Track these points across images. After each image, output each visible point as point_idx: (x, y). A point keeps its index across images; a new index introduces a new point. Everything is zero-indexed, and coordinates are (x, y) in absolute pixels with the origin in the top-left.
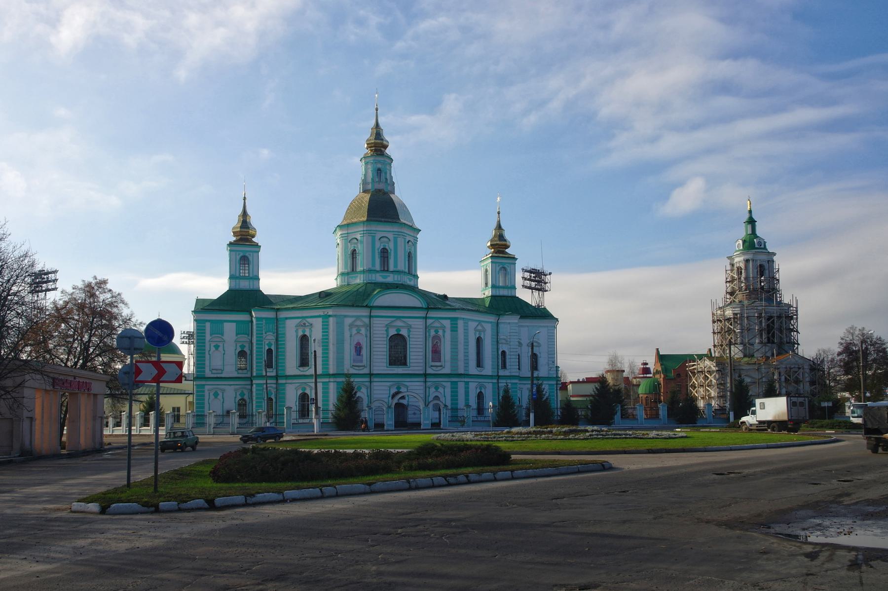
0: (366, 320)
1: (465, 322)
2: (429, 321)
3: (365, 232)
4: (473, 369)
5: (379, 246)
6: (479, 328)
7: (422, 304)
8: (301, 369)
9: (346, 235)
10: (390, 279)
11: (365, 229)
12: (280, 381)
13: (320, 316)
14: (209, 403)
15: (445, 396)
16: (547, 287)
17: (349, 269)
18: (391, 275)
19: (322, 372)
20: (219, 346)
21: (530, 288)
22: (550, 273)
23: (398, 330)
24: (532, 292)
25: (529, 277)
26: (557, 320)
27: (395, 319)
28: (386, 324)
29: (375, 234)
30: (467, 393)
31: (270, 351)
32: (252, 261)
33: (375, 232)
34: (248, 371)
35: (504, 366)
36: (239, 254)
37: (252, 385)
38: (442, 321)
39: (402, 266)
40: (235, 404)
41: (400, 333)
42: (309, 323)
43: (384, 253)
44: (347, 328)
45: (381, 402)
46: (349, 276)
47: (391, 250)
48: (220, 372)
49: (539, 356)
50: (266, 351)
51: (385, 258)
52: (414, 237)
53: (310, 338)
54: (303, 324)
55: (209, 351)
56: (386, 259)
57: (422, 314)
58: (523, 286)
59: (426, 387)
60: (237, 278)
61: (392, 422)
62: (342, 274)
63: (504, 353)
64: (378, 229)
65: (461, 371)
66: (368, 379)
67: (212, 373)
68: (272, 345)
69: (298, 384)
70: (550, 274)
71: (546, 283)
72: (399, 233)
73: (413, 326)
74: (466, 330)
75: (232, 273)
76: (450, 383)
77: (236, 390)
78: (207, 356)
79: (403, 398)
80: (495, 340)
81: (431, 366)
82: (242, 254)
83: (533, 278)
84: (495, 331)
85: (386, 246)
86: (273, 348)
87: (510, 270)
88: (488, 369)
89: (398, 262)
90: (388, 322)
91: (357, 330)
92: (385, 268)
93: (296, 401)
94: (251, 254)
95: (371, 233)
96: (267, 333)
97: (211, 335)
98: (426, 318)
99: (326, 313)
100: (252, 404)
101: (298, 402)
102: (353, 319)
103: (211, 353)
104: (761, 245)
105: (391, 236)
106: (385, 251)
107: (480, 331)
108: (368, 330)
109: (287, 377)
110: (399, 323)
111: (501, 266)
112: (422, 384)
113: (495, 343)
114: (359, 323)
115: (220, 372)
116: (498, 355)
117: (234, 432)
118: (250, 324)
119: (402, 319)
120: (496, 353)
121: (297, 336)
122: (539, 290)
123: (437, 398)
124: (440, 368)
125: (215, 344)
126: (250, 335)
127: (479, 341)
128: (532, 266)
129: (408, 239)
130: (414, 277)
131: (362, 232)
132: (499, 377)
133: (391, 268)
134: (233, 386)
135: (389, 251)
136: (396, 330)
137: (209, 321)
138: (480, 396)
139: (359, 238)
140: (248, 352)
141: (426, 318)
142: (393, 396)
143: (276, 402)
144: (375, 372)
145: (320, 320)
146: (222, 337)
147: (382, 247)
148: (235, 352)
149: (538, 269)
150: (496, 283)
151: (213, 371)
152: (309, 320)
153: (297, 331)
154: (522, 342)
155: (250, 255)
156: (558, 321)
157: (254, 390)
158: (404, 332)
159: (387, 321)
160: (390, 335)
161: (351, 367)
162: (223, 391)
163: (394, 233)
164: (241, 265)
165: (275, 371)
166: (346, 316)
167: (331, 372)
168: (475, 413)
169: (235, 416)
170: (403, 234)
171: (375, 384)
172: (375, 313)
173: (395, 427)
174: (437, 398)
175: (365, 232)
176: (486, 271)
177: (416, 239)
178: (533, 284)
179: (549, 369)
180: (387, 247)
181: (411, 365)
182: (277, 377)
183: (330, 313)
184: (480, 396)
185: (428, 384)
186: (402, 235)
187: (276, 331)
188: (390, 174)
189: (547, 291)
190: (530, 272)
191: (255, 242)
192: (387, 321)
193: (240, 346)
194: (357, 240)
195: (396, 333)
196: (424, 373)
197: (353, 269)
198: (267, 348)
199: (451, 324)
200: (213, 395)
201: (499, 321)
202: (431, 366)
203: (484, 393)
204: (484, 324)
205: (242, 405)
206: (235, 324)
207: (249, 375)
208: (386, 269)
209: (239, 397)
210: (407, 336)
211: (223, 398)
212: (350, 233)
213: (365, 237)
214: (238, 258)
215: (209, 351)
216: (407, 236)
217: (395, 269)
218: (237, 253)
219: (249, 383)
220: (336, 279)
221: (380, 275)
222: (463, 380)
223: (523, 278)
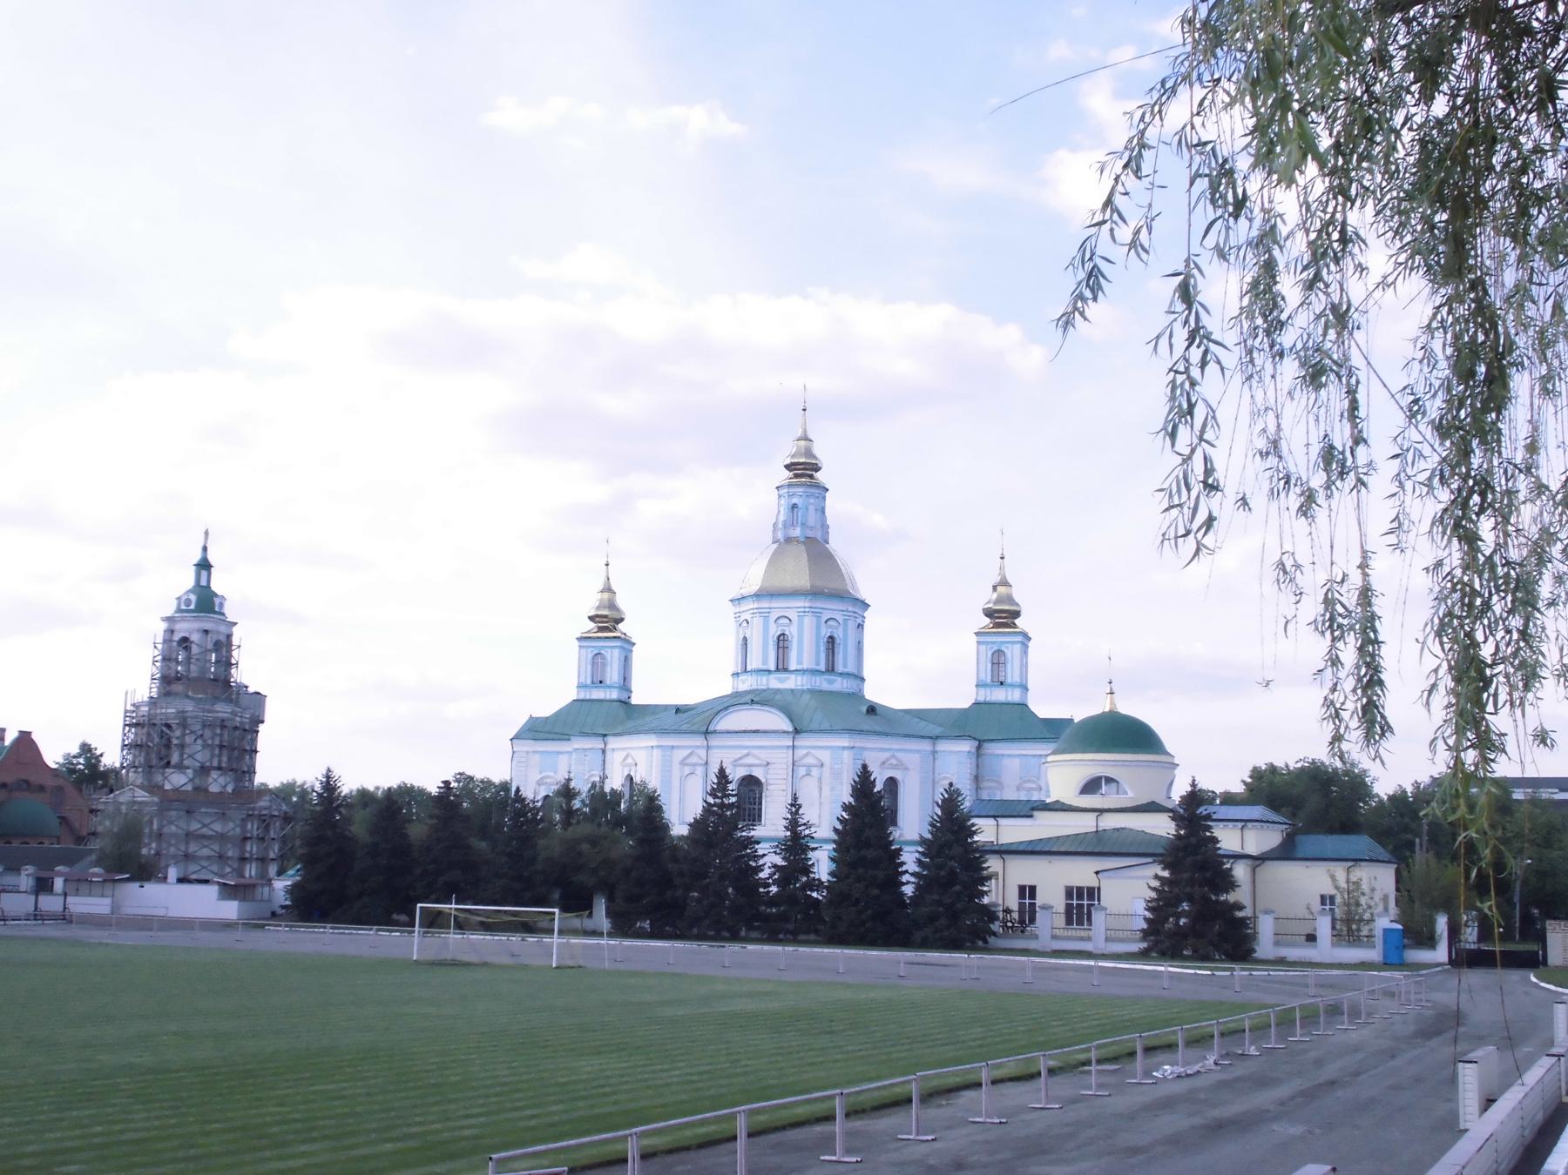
0: (703, 753)
2: (799, 753)
5: (774, 631)
18: (793, 677)
43: (782, 642)
47: (793, 637)
105: (793, 615)
114: (694, 760)
147: (779, 633)
153: (623, 771)
158: (758, 773)
214: (590, 656)
217: (799, 667)
218: (590, 650)
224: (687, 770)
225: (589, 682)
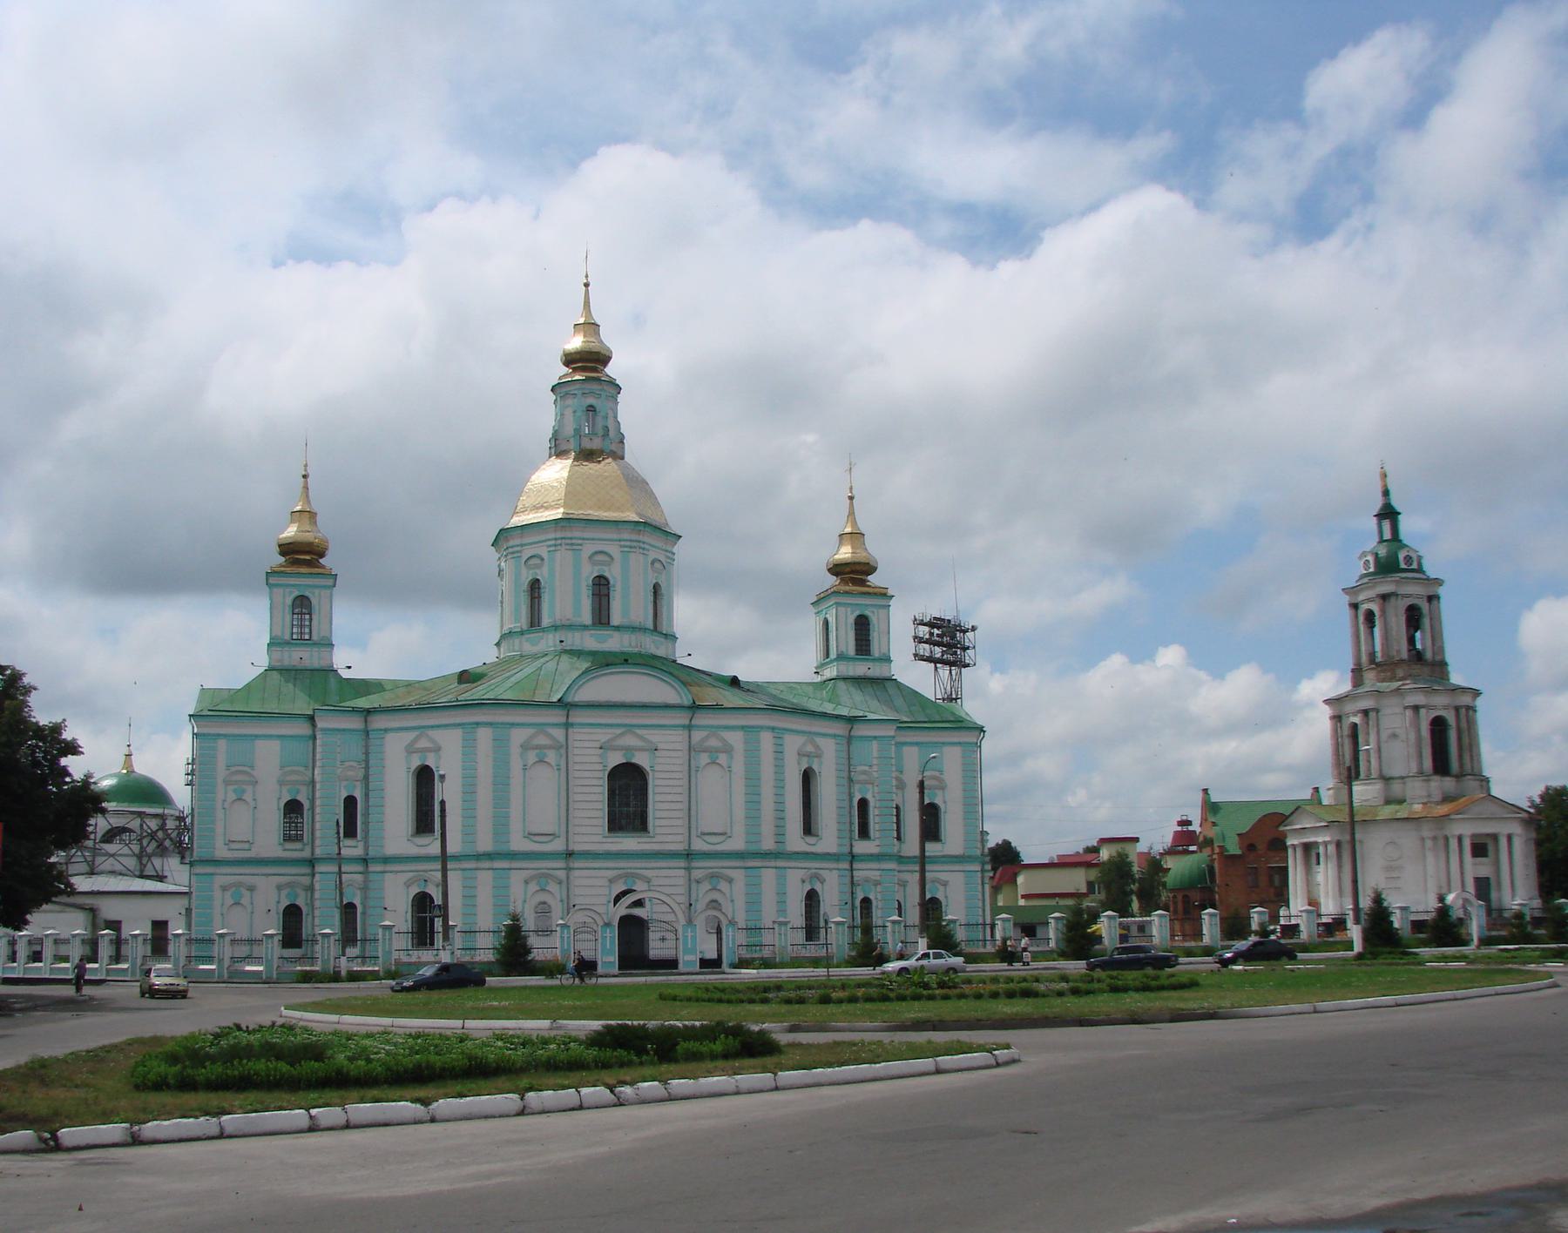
0: (559, 734)
1: (776, 735)
2: (697, 736)
3: (559, 542)
4: (795, 840)
5: (589, 572)
6: (810, 748)
7: (681, 698)
9: (519, 548)
10: (614, 642)
11: (559, 535)
12: (373, 868)
15: (732, 901)
16: (967, 658)
17: (524, 622)
18: (616, 634)
20: (244, 791)
21: (930, 659)
22: (973, 627)
23: (628, 749)
24: (936, 668)
25: (927, 636)
26: (981, 730)
27: (619, 731)
28: (604, 739)
29: (581, 545)
30: (781, 895)
31: (350, 802)
32: (317, 607)
33: (580, 542)
34: (304, 845)
35: (864, 832)
36: (291, 592)
37: (313, 875)
39: (641, 612)
41: (633, 761)
43: (601, 587)
45: (588, 913)
46: (524, 637)
48: (246, 846)
49: (943, 811)
51: (603, 598)
52: (666, 551)
55: (224, 801)
56: (604, 600)
57: (681, 718)
58: (916, 655)
59: (690, 880)
60: (287, 643)
61: (614, 958)
62: (506, 636)
63: (863, 804)
64: (587, 535)
65: (768, 844)
66: (561, 864)
68: (355, 786)
69: (412, 874)
70: (974, 629)
71: (965, 649)
72: (635, 544)
73: (660, 746)
74: (779, 752)
75: (273, 635)
77: (279, 888)
78: (220, 814)
79: (639, 903)
80: (845, 774)
81: (704, 834)
82: (297, 593)
83: (937, 639)
84: (845, 755)
85: (604, 571)
86: (358, 794)
87: (878, 619)
88: (830, 836)
89: (628, 605)
90: (609, 736)
91: (537, 755)
92: (601, 616)
93: (406, 912)
94: (317, 591)
95: (572, 544)
96: (347, 764)
97: (228, 766)
98: (689, 727)
100: (313, 917)
101: (409, 914)
102: (531, 731)
104: (1411, 564)
105: (613, 550)
106: (603, 582)
107: (808, 755)
108: (561, 756)
109: (386, 860)
111: (857, 613)
113: (845, 782)
114: (542, 740)
115: (246, 846)
116: (851, 807)
117: (271, 978)
118: (311, 742)
119: (639, 731)
120: (846, 804)
122: (951, 664)
123: (714, 904)
127: (808, 777)
128: (934, 611)
129: (652, 555)
130: (666, 638)
131: (553, 542)
132: (853, 857)
133: (616, 620)
135: (612, 582)
137: (225, 736)
138: (812, 898)
139: (545, 555)
140: (306, 805)
141: (689, 727)
142: (617, 899)
143: (364, 913)
144: (577, 848)
145: (458, 732)
146: (254, 773)
149: (947, 618)
150: (847, 650)
151: (233, 846)
154: (904, 777)
155: (313, 594)
156: (984, 732)
157: (317, 886)
158: (641, 759)
159: (603, 736)
160: (609, 769)
163: (622, 543)
164: (295, 616)
165: (361, 845)
166: (513, 725)
168: (800, 936)
169: (272, 943)
170: (642, 546)
171: (577, 873)
172: (578, 717)
173: (619, 969)
174: (714, 904)
175: (559, 542)
176: (826, 623)
177: (671, 556)
178: (938, 651)
180: (606, 574)
181: (658, 830)
182: (365, 861)
184: (812, 898)
185: (697, 874)
186: (640, 548)
188: (616, 417)
189: (968, 666)
190: (931, 625)
191: (323, 567)
192: (603, 736)
193: (289, 791)
194: (542, 559)
195: (624, 761)
197: (535, 621)
198: (345, 794)
199: (746, 742)
201: (852, 734)
202: (704, 834)
203: (820, 893)
204: (819, 740)
205: (292, 915)
207: (306, 854)
208: (604, 620)
209: (285, 903)
210: (648, 769)
212: (525, 545)
213: (558, 554)
214: (289, 601)
215: (224, 801)
216: (650, 548)
219: (307, 870)
220: (498, 644)
221: (592, 636)
222: (773, 864)
223: (915, 637)
224: (532, 757)
225: (287, 637)
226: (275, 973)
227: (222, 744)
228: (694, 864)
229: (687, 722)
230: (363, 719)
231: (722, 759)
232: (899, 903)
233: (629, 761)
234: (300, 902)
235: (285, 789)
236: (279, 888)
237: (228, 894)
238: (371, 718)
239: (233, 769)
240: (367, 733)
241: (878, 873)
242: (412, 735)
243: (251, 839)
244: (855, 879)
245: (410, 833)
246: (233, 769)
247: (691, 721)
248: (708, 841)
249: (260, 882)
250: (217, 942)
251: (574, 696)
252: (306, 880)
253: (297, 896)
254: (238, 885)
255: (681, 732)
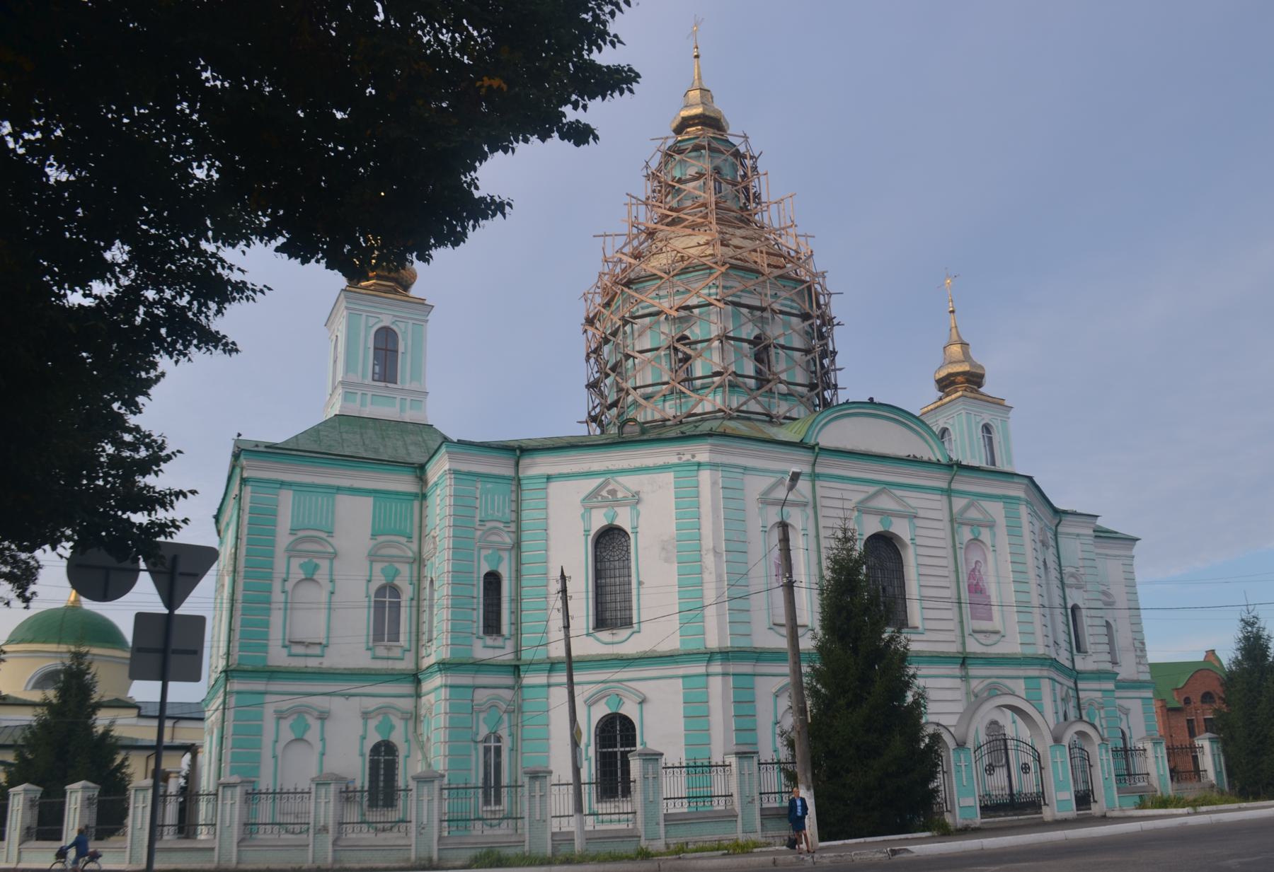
2: (959, 503)
8: (605, 635)
12: (529, 679)
13: (665, 468)
14: (275, 757)
19: (682, 643)
20: (316, 567)
37: (418, 695)
38: (986, 504)
40: (359, 759)
42: (627, 489)
44: (753, 507)
48: (317, 650)
50: (482, 579)
53: (632, 536)
54: (609, 492)
55: (285, 581)
67: (290, 655)
68: (500, 559)
73: (921, 513)
76: (1021, 683)
77: (366, 715)
78: (278, 597)
81: (975, 631)
86: (505, 571)
96: (489, 525)
97: (293, 531)
98: (949, 492)
99: (685, 458)
103: (289, 586)
110: (885, 503)
112: (957, 683)
121: (587, 531)
124: (995, 638)
125: (306, 560)
126: (416, 539)
134: (357, 699)
136: (881, 522)
148: (368, 589)
152: (631, 482)
153: (586, 517)
158: (901, 529)
161: (770, 629)
162: (323, 717)
165: (510, 646)
167: (713, 643)
179: (1138, 660)
183: (703, 457)
185: (976, 685)
187: (514, 516)
192: (856, 495)
196: (961, 650)
198: (485, 569)
200: (291, 727)
206: (369, 501)
207: (407, 665)
209: (375, 738)
211: (323, 739)
226: (435, 847)
227: (286, 499)
228: (973, 671)
229: (944, 485)
230: (513, 462)
231: (985, 535)
232: (1123, 732)
233: (887, 529)
234: (397, 738)
235: (378, 567)
236: (366, 715)
237: (285, 725)
238: (525, 462)
239: (301, 534)
240: (518, 481)
241: (1099, 694)
242: (595, 482)
243: (324, 642)
244: (1081, 702)
245: (591, 626)
246: (301, 534)
247: (950, 483)
248: (982, 641)
249: (336, 704)
250: (414, 793)
251: (816, 439)
252: (407, 704)
253: (392, 728)
254: (300, 712)
255: (938, 497)
